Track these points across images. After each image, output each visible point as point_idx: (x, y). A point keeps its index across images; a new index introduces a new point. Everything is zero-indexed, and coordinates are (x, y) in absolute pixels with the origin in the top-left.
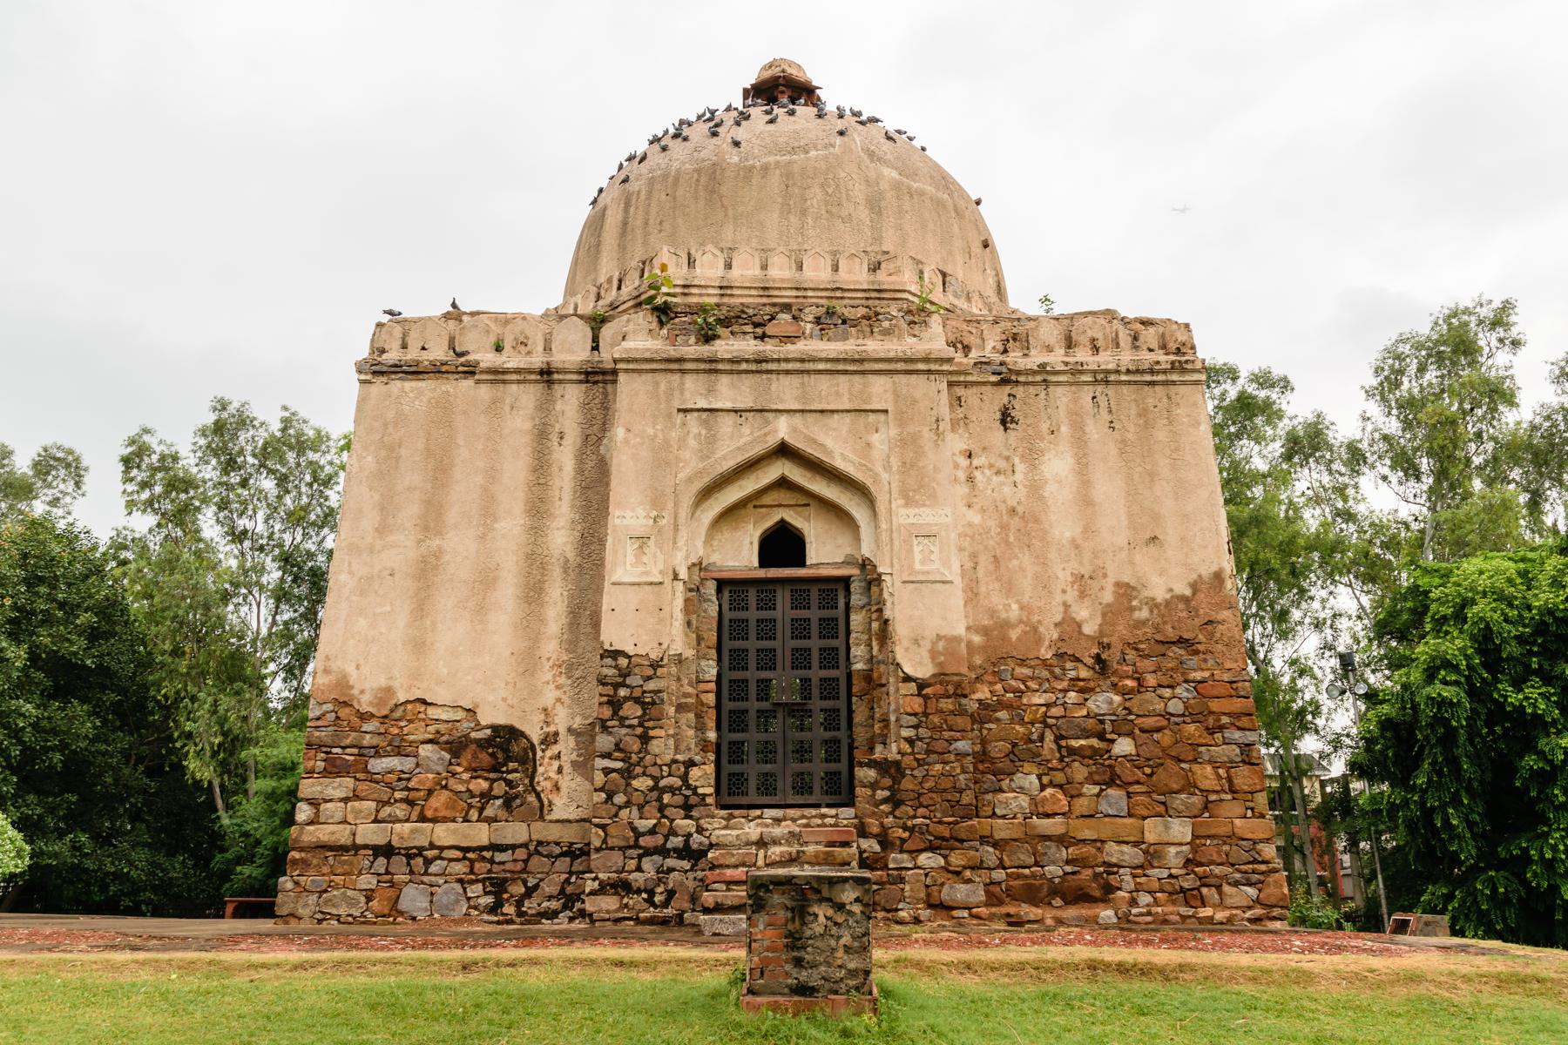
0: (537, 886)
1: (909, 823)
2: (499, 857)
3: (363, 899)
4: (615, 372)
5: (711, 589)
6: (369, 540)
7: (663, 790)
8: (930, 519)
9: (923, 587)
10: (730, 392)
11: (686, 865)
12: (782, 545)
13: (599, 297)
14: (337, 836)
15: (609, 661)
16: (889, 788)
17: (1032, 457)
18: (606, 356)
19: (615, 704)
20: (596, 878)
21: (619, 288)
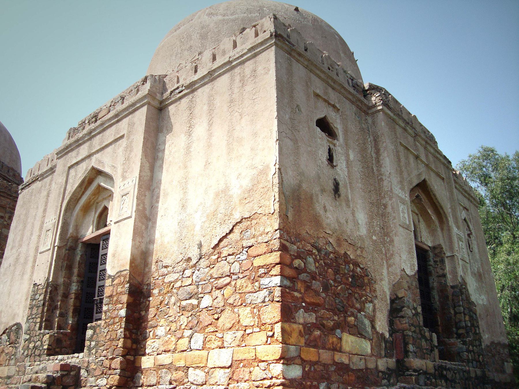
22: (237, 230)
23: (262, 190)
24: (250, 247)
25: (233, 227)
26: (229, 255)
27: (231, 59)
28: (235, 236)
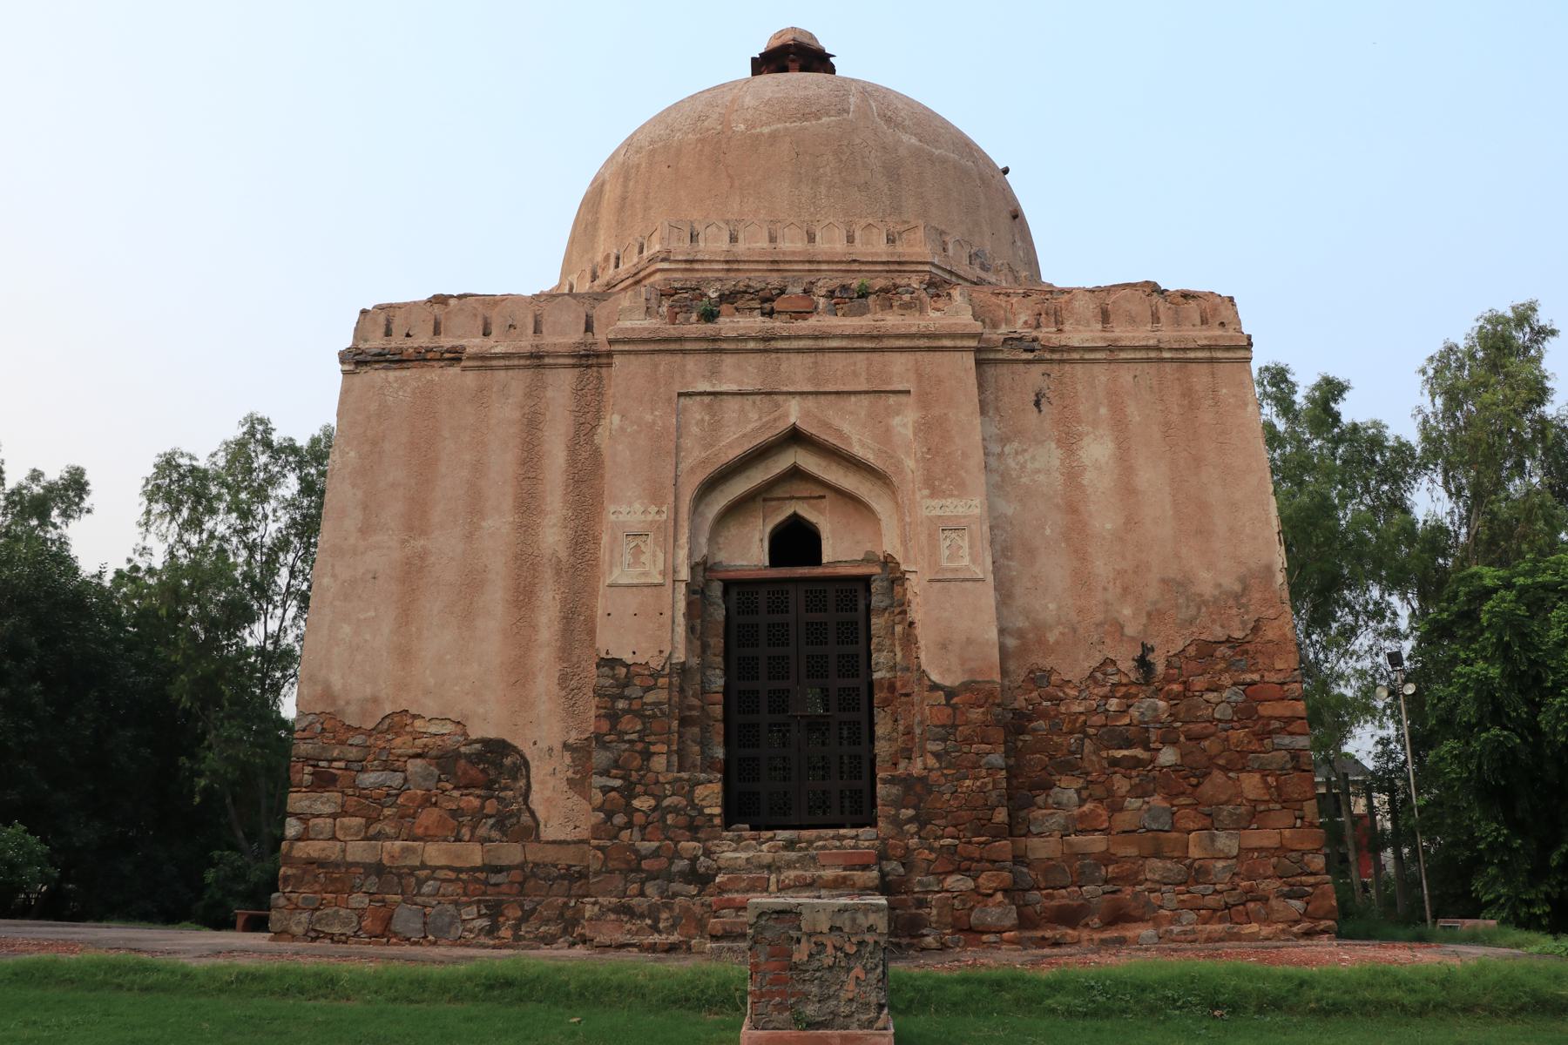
0: (534, 910)
1: (936, 845)
2: (494, 879)
3: (355, 919)
4: (610, 354)
5: (716, 590)
6: (352, 541)
7: (669, 810)
8: (961, 511)
10: (736, 374)
11: (693, 890)
12: (796, 542)
13: (594, 277)
14: (328, 852)
15: (605, 670)
16: (914, 808)
17: (1069, 442)
18: (601, 337)
19: (613, 717)
20: (594, 904)
21: (617, 266)
24: (1249, 685)
26: (1208, 690)
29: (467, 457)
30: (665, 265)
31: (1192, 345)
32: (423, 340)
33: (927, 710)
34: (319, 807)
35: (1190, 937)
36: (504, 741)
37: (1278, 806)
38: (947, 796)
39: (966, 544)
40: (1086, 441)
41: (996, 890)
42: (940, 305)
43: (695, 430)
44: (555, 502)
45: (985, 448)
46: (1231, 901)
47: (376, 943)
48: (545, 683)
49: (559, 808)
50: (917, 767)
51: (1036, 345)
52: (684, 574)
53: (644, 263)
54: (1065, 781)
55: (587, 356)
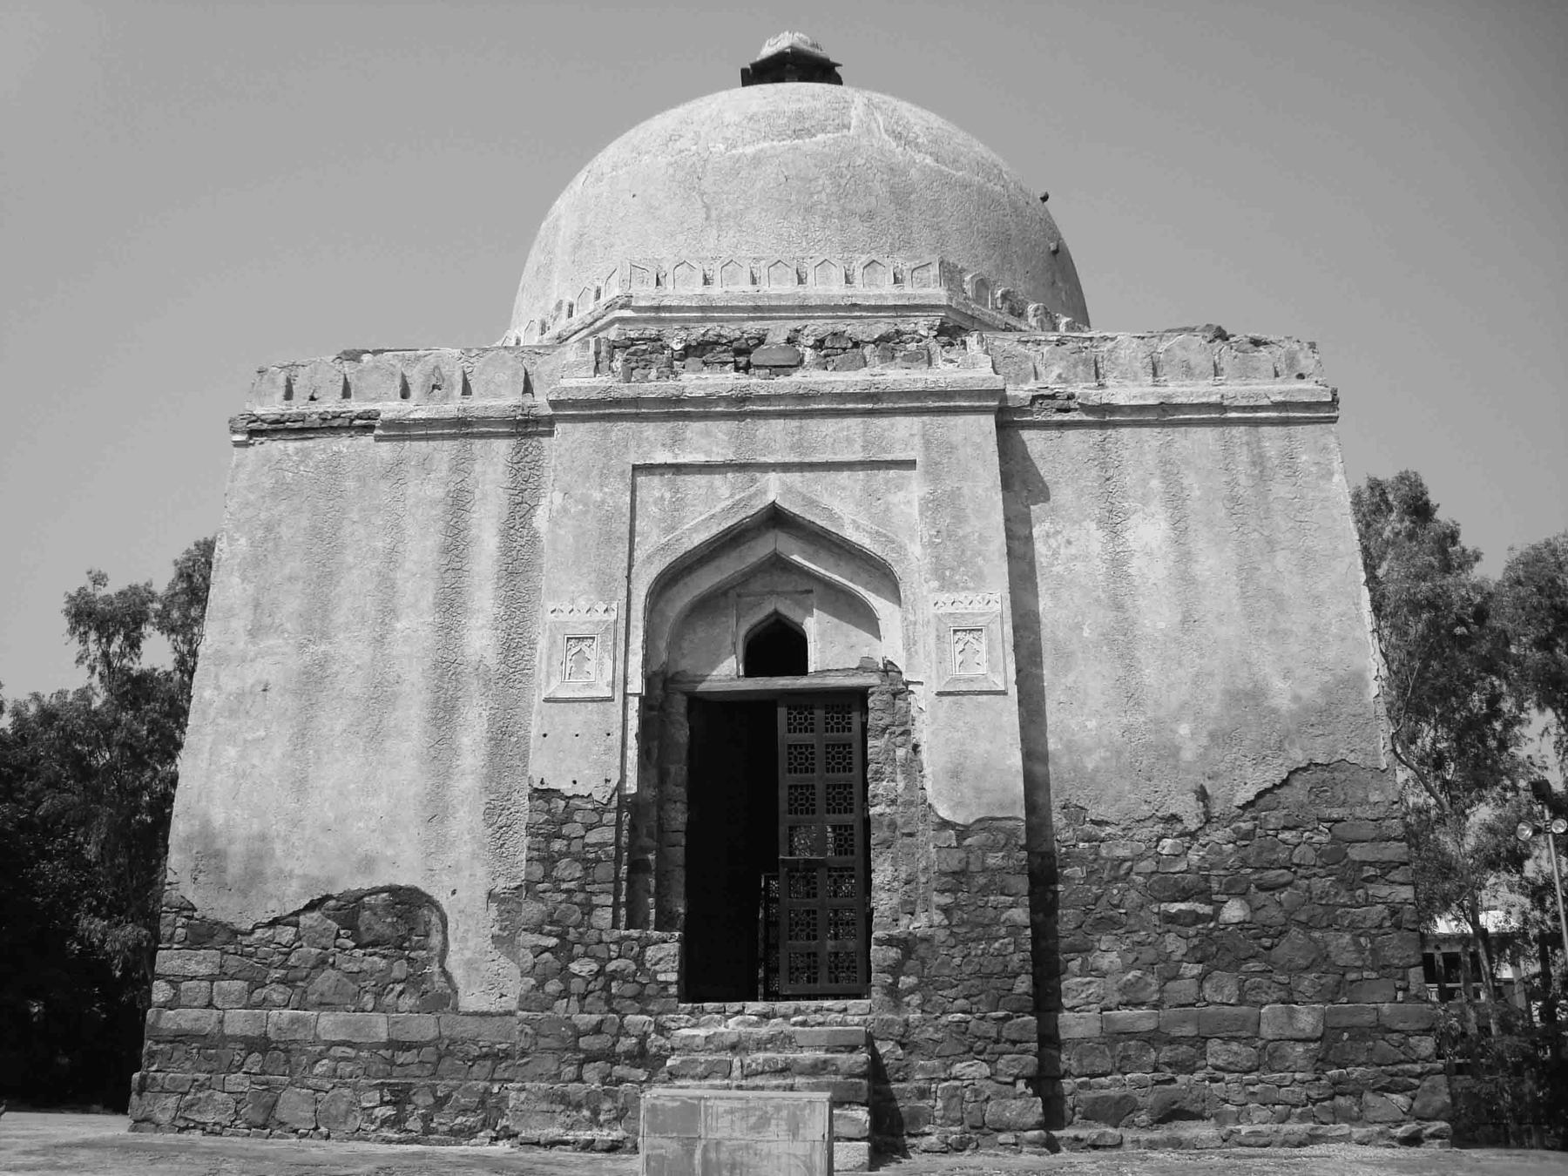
0: (448, 1096)
2: (402, 1057)
3: (232, 1104)
4: (551, 421)
5: (680, 705)
7: (613, 976)
8: (977, 608)
9: (965, 699)
10: (707, 441)
11: (641, 1074)
12: (778, 647)
13: (544, 328)
17: (1113, 522)
18: (541, 403)
19: (549, 861)
21: (570, 315)
22: (1297, 782)
23: (1351, 719)
24: (1336, 821)
25: (1290, 773)
26: (1285, 828)
27: (1226, 403)
28: (1297, 793)
29: (380, 544)
30: (627, 313)
31: (1265, 402)
32: (330, 404)
33: (931, 853)
34: (192, 967)
35: (1262, 1141)
36: (413, 891)
37: (1374, 975)
38: (957, 961)
39: (983, 648)
40: (1134, 520)
41: (1017, 1078)
42: (951, 357)
43: (654, 509)
44: (484, 600)
45: (1008, 530)
46: (1314, 1094)
47: (258, 1136)
48: (466, 821)
49: (483, 974)
50: (919, 924)
51: (1072, 404)
52: (637, 685)
53: (601, 310)
54: (1105, 941)
55: (526, 422)
